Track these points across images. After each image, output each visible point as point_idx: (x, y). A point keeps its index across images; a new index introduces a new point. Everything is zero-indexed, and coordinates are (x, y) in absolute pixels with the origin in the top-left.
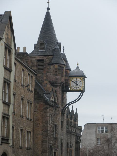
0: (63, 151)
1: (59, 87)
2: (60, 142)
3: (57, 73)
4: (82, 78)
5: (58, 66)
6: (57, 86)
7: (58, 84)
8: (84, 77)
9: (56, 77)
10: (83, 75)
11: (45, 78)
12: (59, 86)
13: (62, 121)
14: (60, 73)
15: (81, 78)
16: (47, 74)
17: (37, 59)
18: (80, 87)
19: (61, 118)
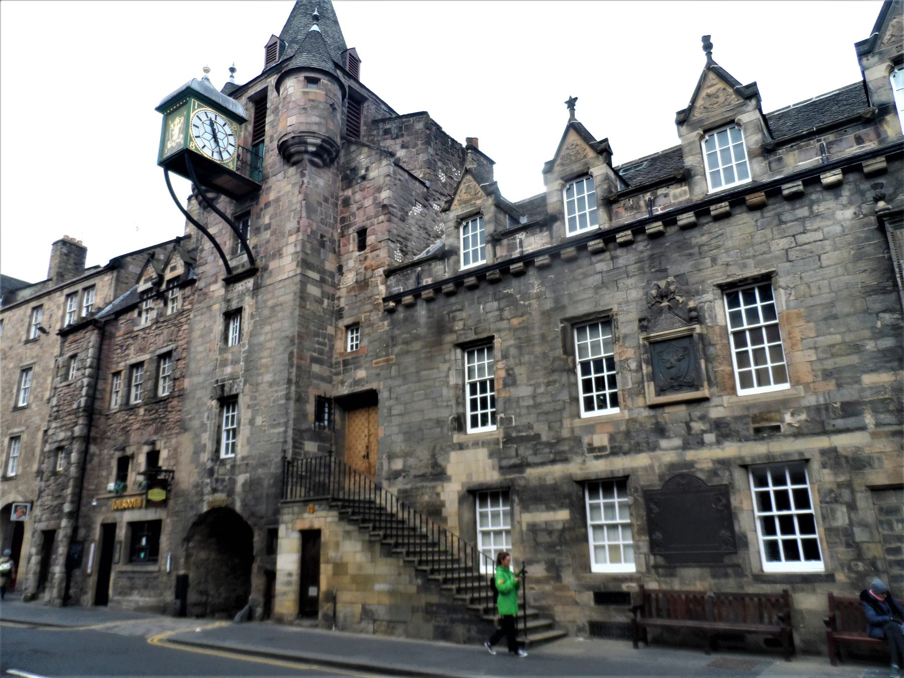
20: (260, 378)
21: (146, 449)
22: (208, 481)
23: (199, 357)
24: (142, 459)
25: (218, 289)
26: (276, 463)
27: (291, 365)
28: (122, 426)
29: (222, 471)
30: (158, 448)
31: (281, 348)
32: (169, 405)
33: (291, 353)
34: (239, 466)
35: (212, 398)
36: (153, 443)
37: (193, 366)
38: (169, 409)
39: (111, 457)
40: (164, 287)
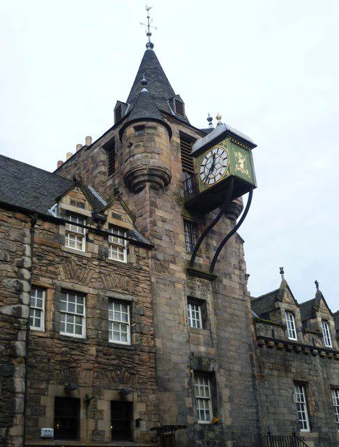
0: (225, 398)
1: (147, 188)
2: (183, 366)
3: (132, 147)
4: (224, 142)
5: (137, 129)
6: (141, 186)
7: (142, 179)
8: (247, 146)
9: (132, 159)
10: (224, 130)
11: (117, 182)
12: (148, 184)
13: (198, 295)
14: (141, 144)
15: (222, 144)
16: (122, 167)
17: (103, 144)
18: (223, 171)
19: (180, 286)
20: (232, 365)
21: (109, 395)
22: (200, 442)
23: (168, 323)
24: (104, 406)
25: (178, 271)
26: (255, 435)
27: (253, 366)
28: (59, 358)
29: (211, 435)
30: (130, 398)
31: (244, 350)
32: (137, 358)
33: (251, 356)
34: (226, 433)
35: (190, 367)
36: (123, 394)
37: (163, 330)
38: (137, 362)
39: (43, 392)
40: (105, 227)
